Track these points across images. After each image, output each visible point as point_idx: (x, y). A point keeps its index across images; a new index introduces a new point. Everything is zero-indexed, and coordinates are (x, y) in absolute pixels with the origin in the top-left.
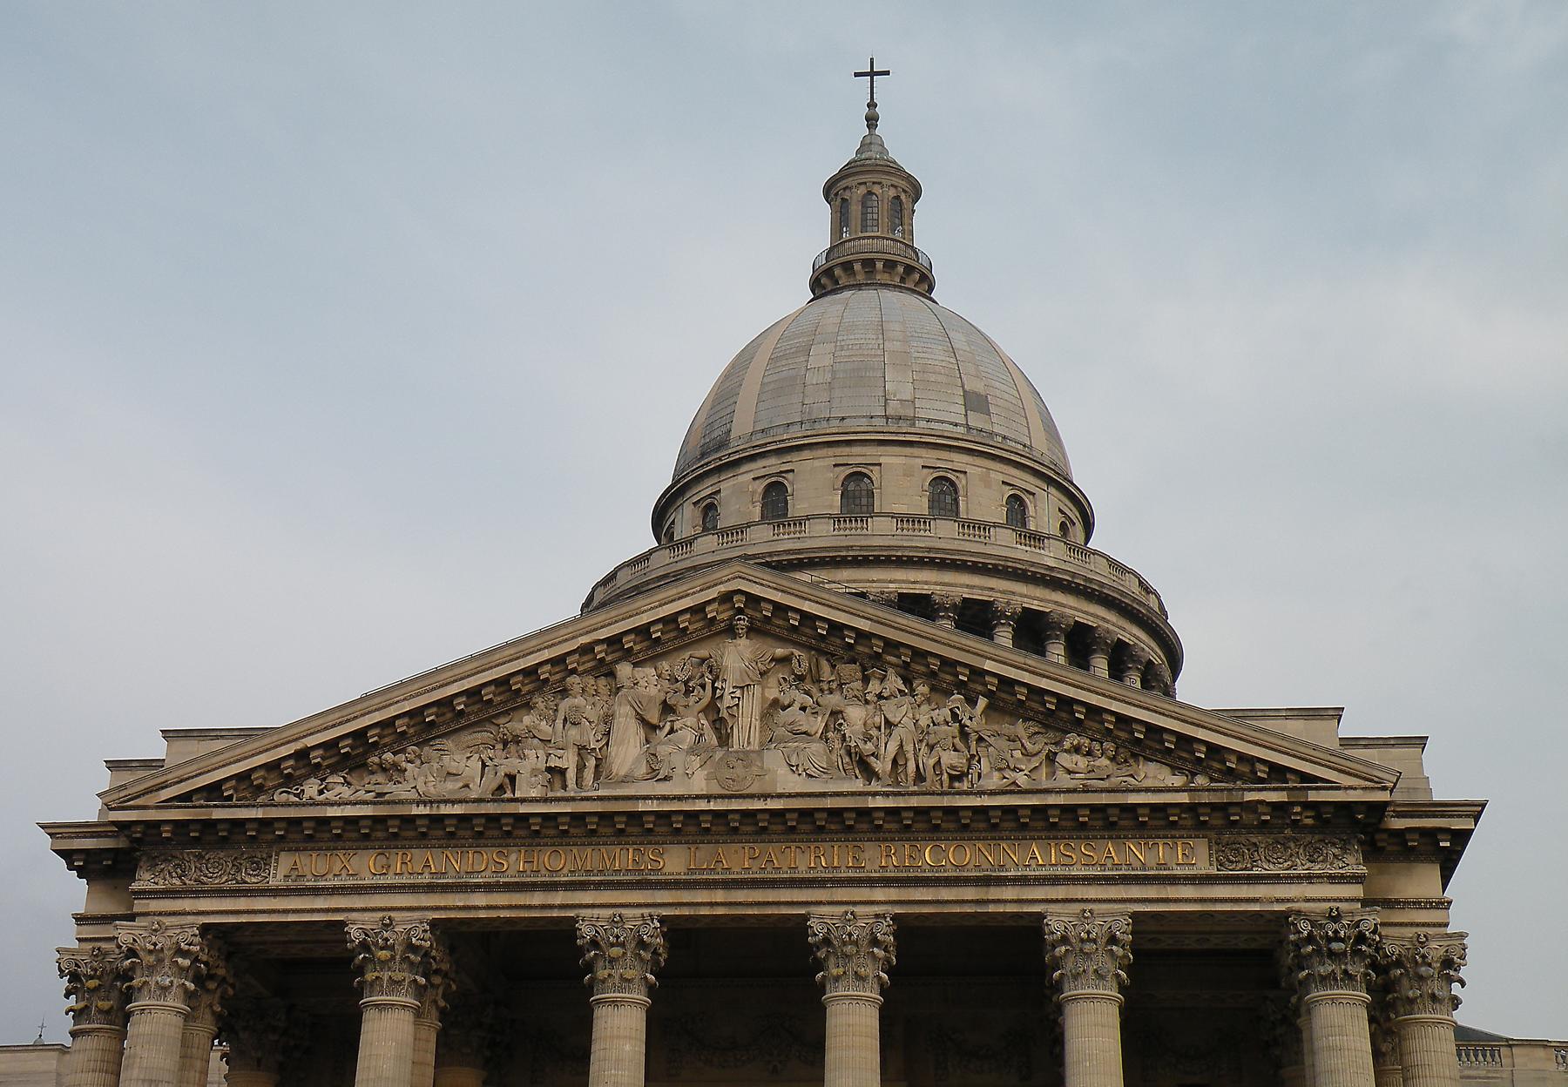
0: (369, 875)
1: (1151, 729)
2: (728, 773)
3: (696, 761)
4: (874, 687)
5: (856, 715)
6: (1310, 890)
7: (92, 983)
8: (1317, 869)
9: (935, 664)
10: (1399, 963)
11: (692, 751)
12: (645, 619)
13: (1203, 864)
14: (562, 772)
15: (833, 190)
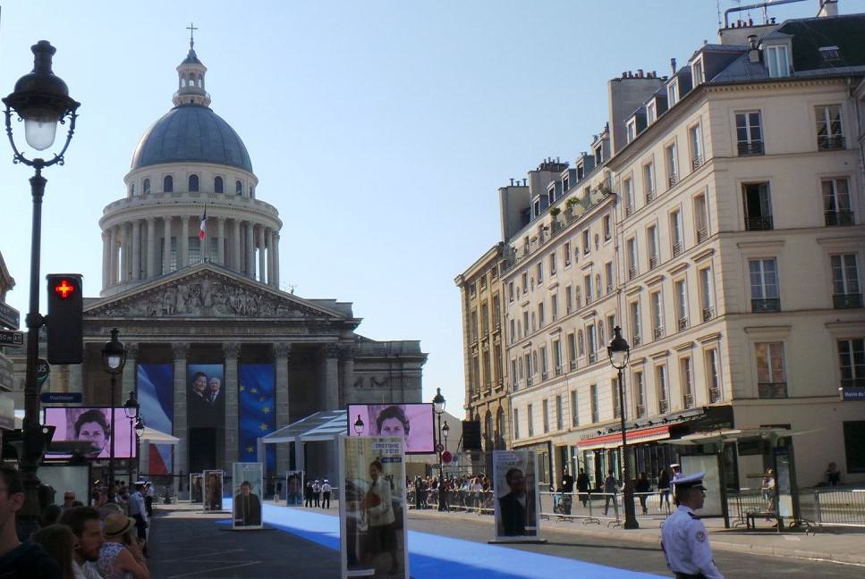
3: (197, 309)
4: (237, 292)
5: (232, 299)
13: (307, 333)
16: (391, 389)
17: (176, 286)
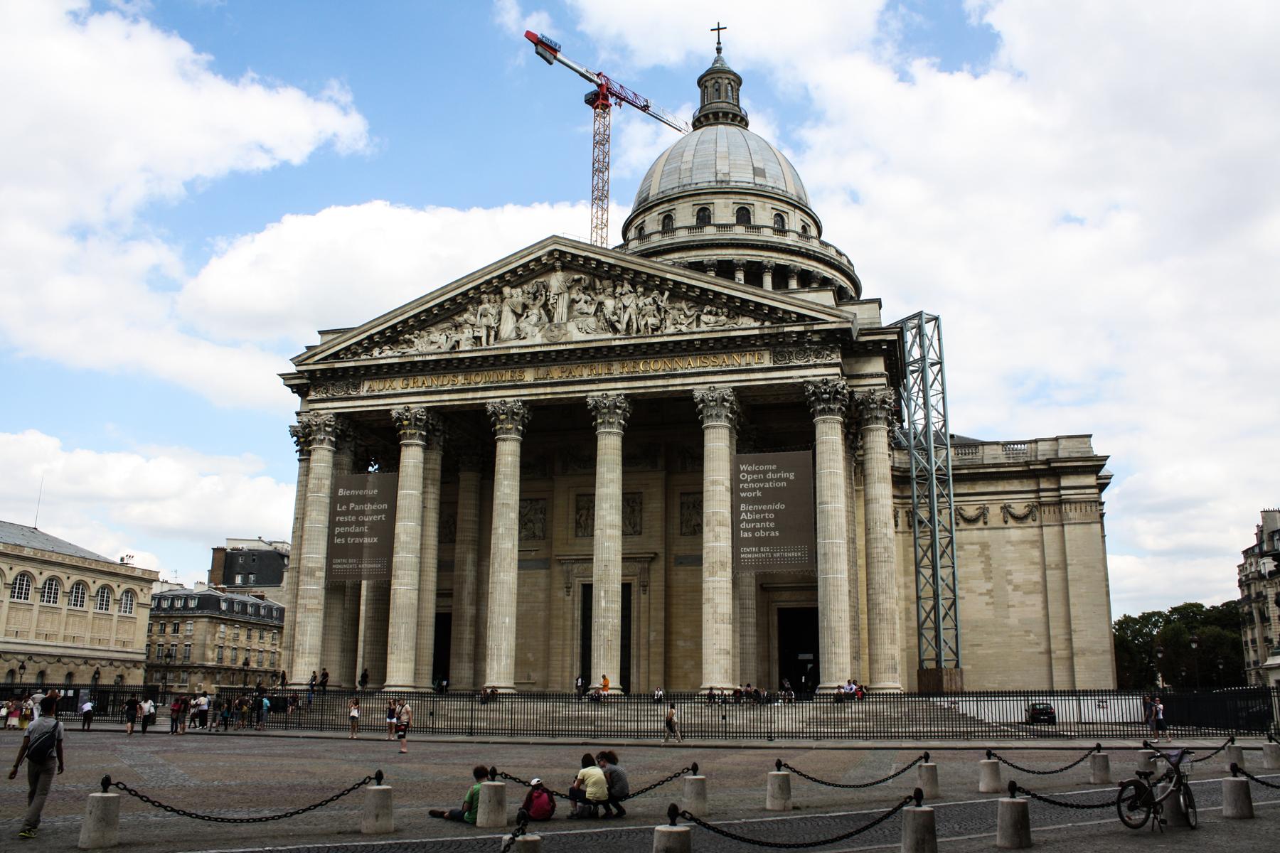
1: (744, 301)
2: (550, 334)
3: (537, 329)
4: (619, 290)
5: (610, 304)
6: (818, 371)
8: (819, 361)
9: (644, 277)
10: (862, 403)
11: (536, 325)
12: (514, 266)
13: (767, 362)
14: (480, 338)
15: (701, 82)
16: (1041, 527)
17: (498, 291)
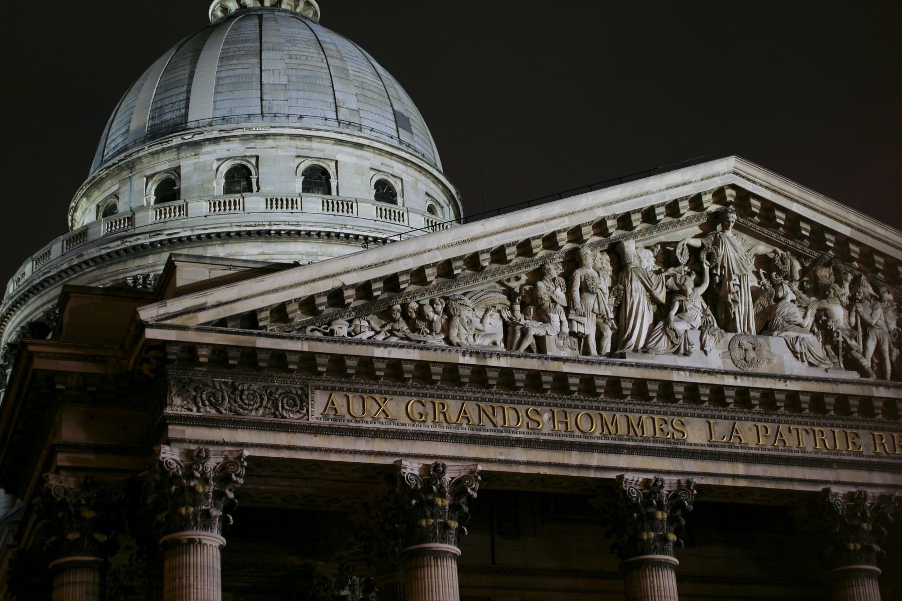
0: (408, 421)
7: (88, 514)
